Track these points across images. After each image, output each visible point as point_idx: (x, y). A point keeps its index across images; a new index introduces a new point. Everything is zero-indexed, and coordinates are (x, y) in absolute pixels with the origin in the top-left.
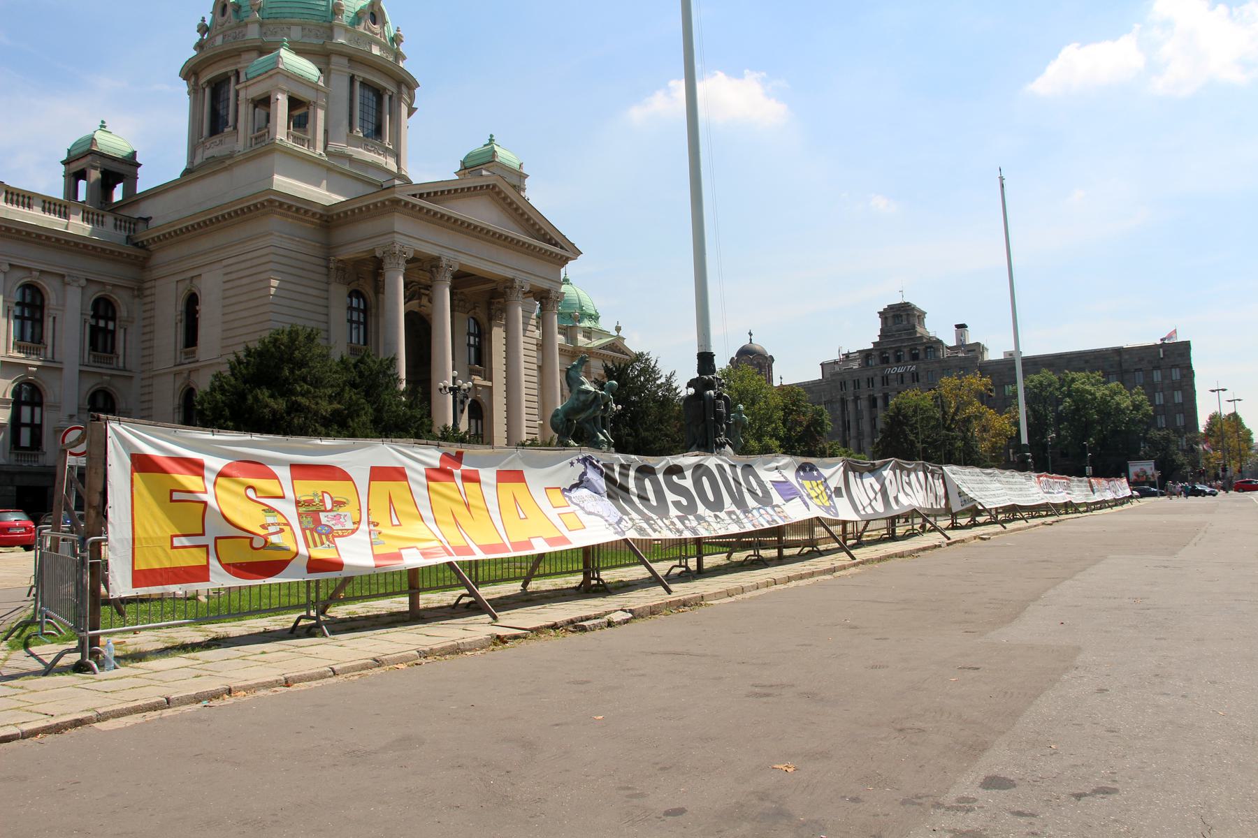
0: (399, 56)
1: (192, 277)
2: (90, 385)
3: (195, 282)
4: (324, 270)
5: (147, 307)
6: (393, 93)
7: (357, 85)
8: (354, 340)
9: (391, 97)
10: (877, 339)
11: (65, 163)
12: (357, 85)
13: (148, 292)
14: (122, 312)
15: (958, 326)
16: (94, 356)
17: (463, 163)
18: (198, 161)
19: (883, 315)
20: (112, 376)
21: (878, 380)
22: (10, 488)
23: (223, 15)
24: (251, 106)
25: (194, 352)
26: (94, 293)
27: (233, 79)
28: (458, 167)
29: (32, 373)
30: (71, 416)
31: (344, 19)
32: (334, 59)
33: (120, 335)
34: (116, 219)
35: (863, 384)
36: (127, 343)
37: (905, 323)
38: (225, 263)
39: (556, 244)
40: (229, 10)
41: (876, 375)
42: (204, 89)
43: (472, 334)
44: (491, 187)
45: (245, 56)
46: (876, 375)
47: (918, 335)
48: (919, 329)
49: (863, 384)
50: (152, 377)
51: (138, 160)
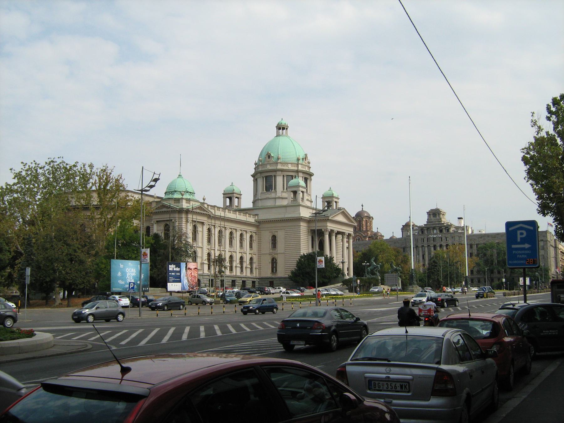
0: (310, 168)
10: (426, 223)
11: (223, 194)
14: (254, 238)
15: (459, 218)
19: (429, 213)
21: (425, 240)
27: (274, 177)
31: (301, 162)
35: (420, 241)
36: (255, 245)
37: (438, 217)
38: (286, 230)
41: (425, 238)
42: (263, 178)
45: (277, 172)
46: (425, 238)
47: (443, 222)
48: (443, 220)
49: (420, 241)
51: (241, 193)
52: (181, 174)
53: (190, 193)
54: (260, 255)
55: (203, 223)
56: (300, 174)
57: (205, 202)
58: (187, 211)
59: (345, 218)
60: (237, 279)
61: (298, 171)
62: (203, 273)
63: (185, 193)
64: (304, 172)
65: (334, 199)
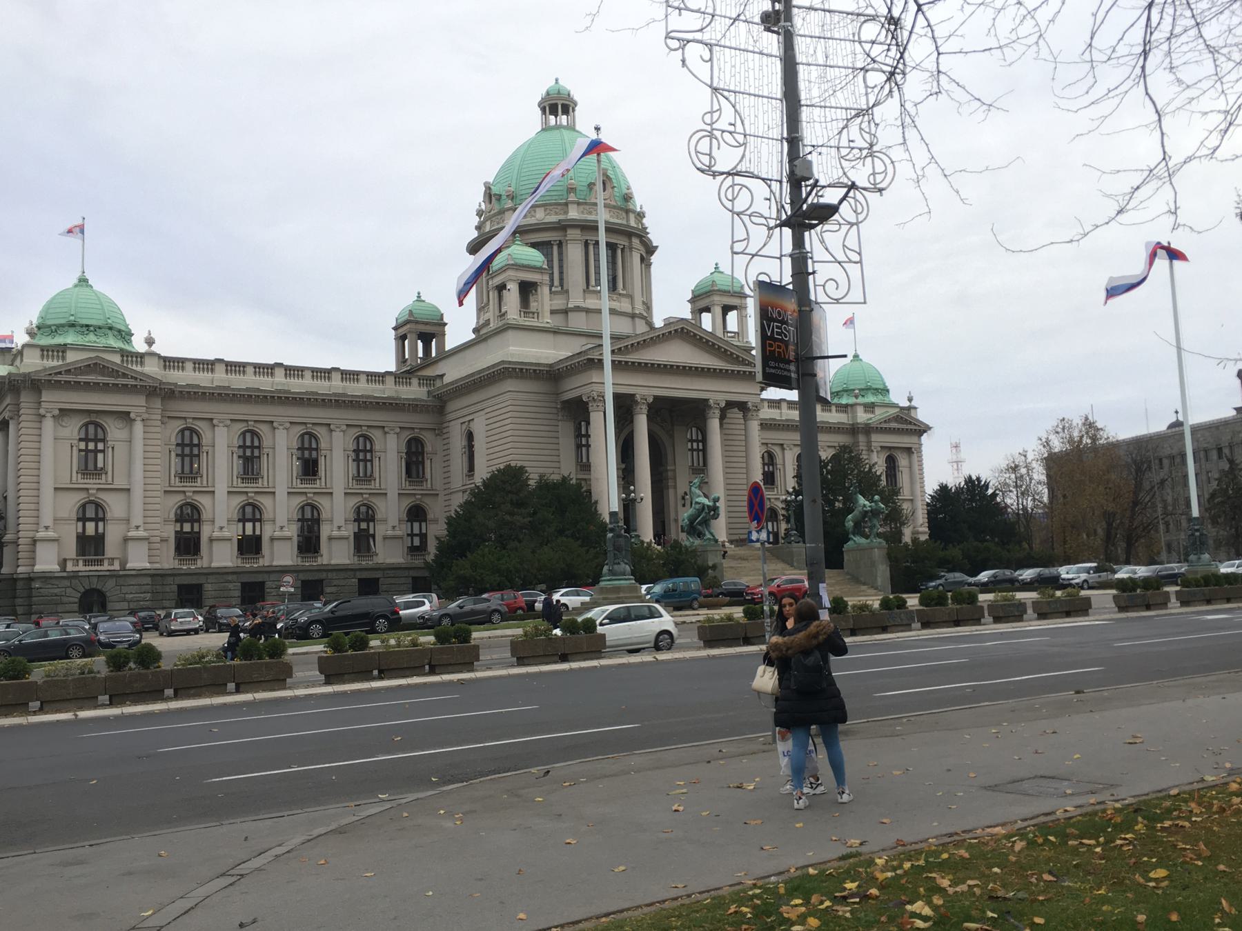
1: (469, 421)
2: (407, 503)
3: (471, 423)
4: (554, 411)
5: (445, 442)
8: (584, 460)
9: (623, 250)
13: (445, 431)
14: (428, 448)
16: (410, 482)
17: (693, 291)
18: (481, 322)
20: (422, 494)
22: (353, 580)
23: (491, 203)
24: (496, 292)
25: (473, 475)
26: (406, 435)
28: (690, 296)
29: (366, 499)
30: (394, 527)
32: (569, 231)
33: (427, 463)
34: (419, 379)
36: (432, 469)
40: (493, 198)
43: (695, 441)
50: (451, 493)
51: (445, 320)
52: (87, 276)
53: (84, 329)
54: (447, 498)
55: (125, 417)
56: (573, 234)
57: (155, 348)
58: (34, 384)
59: (707, 352)
60: (330, 575)
61: (562, 227)
62: (123, 568)
63: (65, 329)
65: (716, 298)
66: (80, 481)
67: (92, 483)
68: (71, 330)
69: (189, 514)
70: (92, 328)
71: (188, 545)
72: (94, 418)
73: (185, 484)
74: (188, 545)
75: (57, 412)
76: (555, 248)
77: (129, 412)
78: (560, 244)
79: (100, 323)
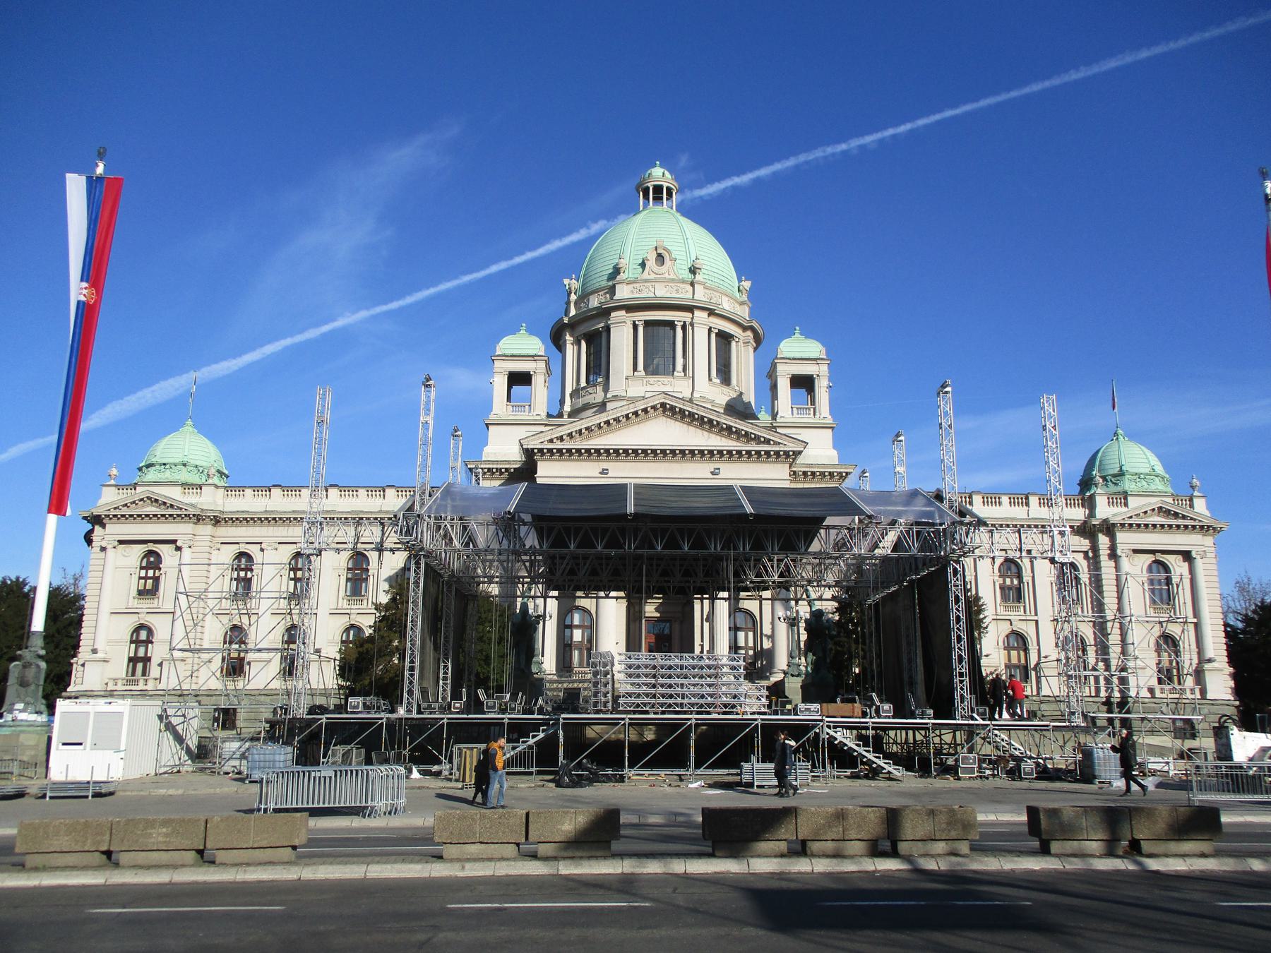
6: (685, 322)
7: (641, 330)
9: (684, 327)
12: (641, 330)
32: (613, 314)
39: (768, 442)
44: (659, 406)
53: (163, 466)
61: (604, 313)
64: (630, 308)
66: (134, 603)
67: (146, 604)
68: (153, 468)
69: (236, 634)
70: (168, 466)
71: (235, 668)
72: (151, 547)
73: (353, 607)
74: (235, 668)
75: (116, 543)
76: (604, 335)
77: (176, 541)
78: (608, 329)
79: (177, 461)
